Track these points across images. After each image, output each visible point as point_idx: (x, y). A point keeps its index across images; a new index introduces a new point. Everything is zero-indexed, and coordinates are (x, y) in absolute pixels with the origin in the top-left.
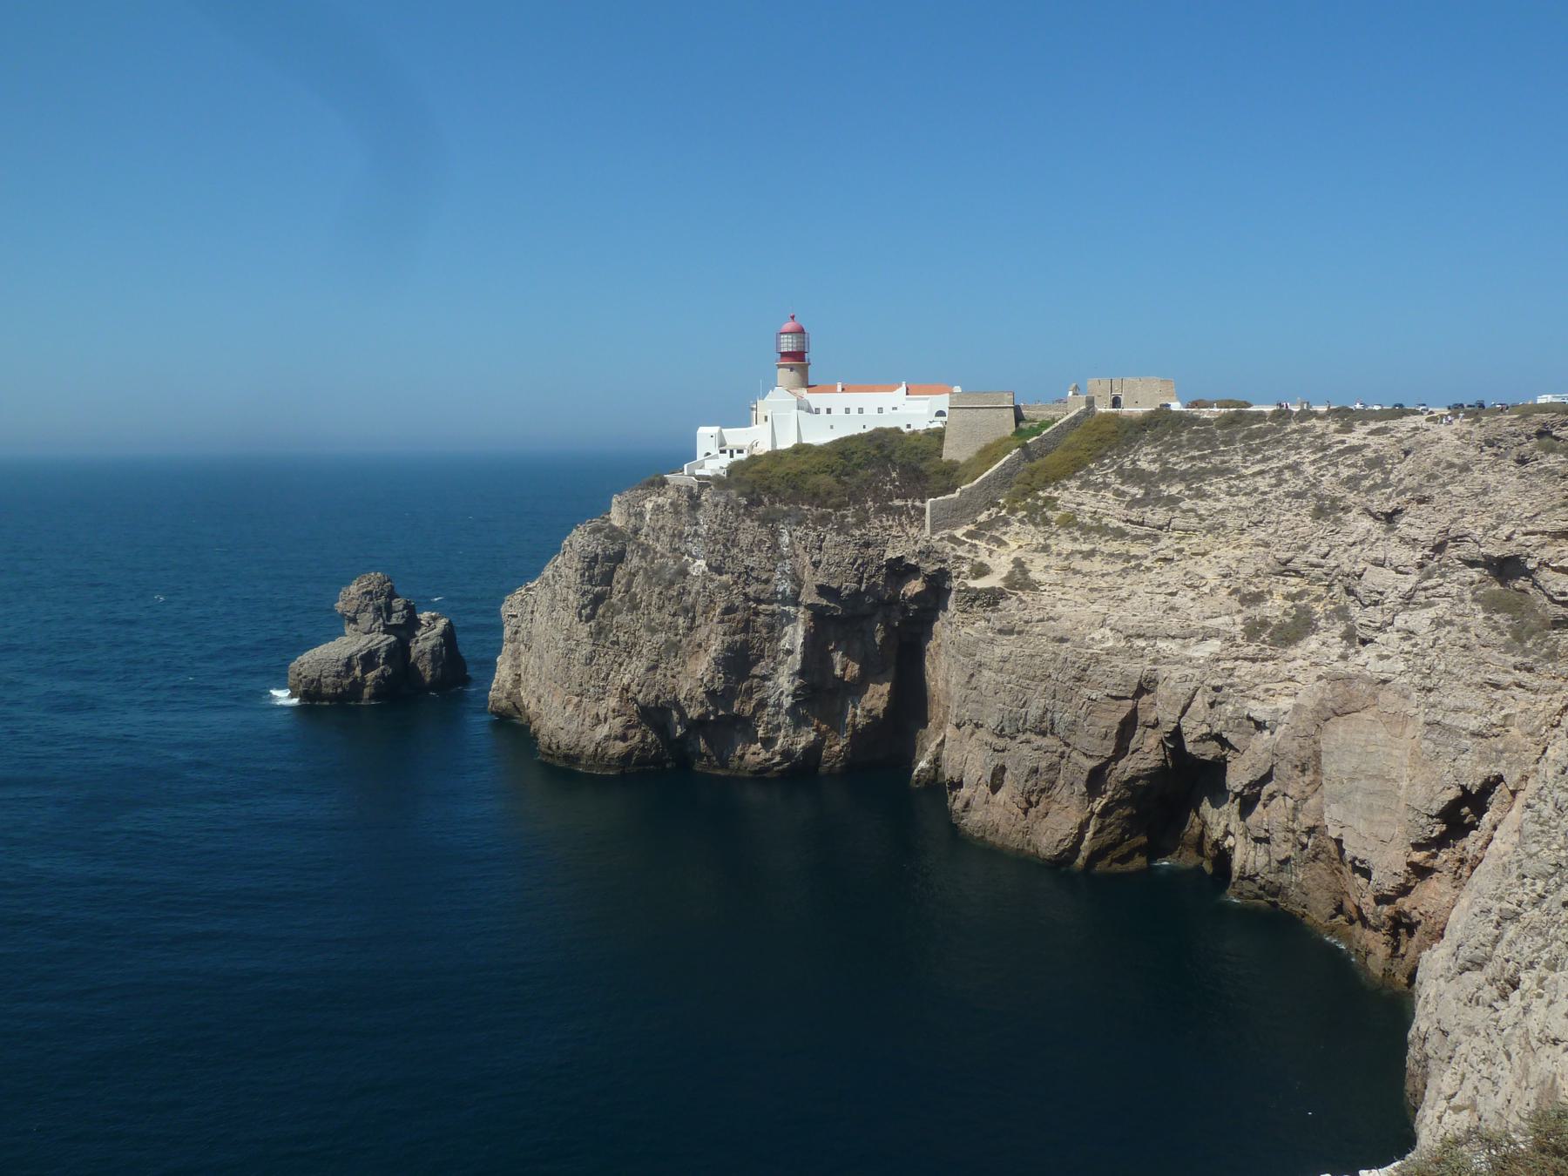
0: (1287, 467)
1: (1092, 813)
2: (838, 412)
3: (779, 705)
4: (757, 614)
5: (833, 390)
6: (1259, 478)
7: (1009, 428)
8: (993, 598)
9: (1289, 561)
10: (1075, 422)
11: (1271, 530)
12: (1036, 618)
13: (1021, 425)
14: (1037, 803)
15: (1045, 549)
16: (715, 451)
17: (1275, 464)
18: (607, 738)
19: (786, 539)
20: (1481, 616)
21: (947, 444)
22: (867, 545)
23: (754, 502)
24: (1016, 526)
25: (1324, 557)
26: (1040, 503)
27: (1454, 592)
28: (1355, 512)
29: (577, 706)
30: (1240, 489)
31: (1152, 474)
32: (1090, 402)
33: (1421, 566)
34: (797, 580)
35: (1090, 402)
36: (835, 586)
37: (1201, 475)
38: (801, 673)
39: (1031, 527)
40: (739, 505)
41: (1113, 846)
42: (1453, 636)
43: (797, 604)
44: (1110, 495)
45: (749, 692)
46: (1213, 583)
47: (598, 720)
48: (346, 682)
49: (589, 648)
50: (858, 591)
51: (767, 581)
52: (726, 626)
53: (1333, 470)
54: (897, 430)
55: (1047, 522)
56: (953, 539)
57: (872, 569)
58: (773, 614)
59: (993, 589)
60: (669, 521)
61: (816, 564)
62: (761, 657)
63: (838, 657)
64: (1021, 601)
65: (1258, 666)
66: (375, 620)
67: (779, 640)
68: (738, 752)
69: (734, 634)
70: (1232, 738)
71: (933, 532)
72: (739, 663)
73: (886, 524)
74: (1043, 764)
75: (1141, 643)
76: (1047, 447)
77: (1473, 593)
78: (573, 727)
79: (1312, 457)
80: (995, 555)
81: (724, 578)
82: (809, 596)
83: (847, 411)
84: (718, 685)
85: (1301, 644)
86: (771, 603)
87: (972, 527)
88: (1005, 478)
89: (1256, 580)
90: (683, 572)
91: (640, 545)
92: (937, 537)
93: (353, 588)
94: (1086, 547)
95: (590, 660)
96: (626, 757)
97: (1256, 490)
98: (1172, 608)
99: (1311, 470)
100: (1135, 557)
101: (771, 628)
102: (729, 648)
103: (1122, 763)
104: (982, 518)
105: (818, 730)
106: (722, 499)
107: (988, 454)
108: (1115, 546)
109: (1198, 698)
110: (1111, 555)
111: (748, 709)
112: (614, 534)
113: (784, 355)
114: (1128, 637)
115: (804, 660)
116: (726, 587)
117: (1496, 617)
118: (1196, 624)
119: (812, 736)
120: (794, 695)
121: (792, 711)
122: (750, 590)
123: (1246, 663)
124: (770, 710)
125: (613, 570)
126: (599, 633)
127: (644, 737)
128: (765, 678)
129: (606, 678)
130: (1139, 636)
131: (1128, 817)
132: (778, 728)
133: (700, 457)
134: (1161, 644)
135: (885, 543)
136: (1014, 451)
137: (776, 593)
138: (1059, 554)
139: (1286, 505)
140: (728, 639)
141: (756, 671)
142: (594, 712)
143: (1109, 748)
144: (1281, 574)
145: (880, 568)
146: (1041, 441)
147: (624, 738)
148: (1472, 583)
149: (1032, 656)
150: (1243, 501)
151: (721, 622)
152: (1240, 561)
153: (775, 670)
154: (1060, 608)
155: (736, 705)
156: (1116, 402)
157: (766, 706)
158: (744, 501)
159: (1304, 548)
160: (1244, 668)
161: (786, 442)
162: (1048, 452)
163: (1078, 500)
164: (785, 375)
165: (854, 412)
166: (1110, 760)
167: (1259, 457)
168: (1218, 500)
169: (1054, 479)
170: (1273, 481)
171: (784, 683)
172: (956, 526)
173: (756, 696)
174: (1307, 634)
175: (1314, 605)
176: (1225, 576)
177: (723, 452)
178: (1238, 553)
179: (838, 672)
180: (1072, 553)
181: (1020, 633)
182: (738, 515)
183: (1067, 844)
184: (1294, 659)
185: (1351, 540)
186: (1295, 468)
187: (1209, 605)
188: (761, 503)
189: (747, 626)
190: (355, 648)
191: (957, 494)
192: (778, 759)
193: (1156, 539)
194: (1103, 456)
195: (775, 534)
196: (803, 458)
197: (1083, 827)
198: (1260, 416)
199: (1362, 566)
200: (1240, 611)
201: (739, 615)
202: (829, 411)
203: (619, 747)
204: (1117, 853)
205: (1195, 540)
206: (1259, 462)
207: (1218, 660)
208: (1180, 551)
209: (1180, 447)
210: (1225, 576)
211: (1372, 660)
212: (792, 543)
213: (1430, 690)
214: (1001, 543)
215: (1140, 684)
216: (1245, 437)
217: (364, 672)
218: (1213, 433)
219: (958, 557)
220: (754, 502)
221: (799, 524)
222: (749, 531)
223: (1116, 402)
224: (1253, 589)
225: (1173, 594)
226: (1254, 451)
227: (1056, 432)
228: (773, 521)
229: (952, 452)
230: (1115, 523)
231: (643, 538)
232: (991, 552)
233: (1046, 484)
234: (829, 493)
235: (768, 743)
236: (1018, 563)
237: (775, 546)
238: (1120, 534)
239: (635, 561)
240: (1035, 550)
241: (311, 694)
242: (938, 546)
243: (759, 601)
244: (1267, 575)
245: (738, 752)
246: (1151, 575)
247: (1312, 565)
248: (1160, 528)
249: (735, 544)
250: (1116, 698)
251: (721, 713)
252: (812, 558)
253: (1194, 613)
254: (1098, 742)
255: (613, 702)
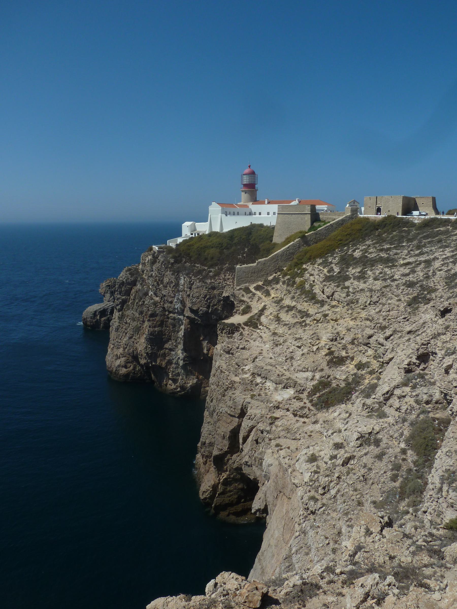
0: (425, 261)
1: (219, 480)
2: (264, 215)
3: (177, 363)
4: (168, 318)
5: (263, 203)
6: (402, 269)
7: (308, 225)
8: (234, 329)
9: (370, 337)
10: (341, 223)
11: (377, 310)
12: (241, 347)
13: (316, 224)
14: (206, 462)
15: (279, 302)
16: (189, 234)
17: (422, 258)
18: (119, 366)
19: (182, 282)
20: (403, 445)
21: (275, 234)
22: (214, 288)
23: (176, 262)
24: (278, 286)
25: (387, 338)
26: (299, 272)
27: (404, 408)
28: (431, 304)
29: (112, 349)
30: (385, 274)
31: (356, 258)
32: (355, 211)
33: (408, 371)
34: (183, 303)
35: (355, 211)
36: (195, 308)
37: (373, 263)
38: (185, 350)
39: (285, 286)
40: (169, 262)
41: (231, 504)
42: (365, 460)
43: (184, 316)
44: (326, 270)
45: (164, 355)
46: (323, 343)
47: (118, 358)
48: (94, 321)
49: (117, 324)
50: (207, 312)
51: (171, 302)
52: (150, 323)
53: (451, 265)
54: (261, 226)
55: (294, 283)
56: (247, 290)
57: (215, 301)
58: (174, 319)
59: (233, 325)
60: (148, 268)
61: (189, 296)
62: (169, 339)
63: (205, 344)
64: (241, 334)
65: (297, 418)
66: (111, 297)
67: (178, 332)
68: (165, 383)
69: (155, 327)
70: (258, 473)
71: (238, 285)
72: (157, 341)
73: (227, 277)
74: (207, 442)
75: (259, 380)
76: (318, 238)
77: (418, 415)
78: (110, 358)
79: (449, 254)
80: (260, 301)
81: (157, 299)
82: (187, 313)
83: (268, 214)
84: (149, 351)
85: (331, 410)
86: (174, 313)
87: (260, 283)
88: (288, 255)
89: (350, 346)
90: (146, 294)
91: (143, 278)
92: (238, 288)
93: (104, 284)
94: (294, 304)
95: (117, 330)
96: (126, 376)
97: (393, 276)
98: (292, 358)
99: (437, 264)
100: (308, 315)
101: (174, 326)
102: (151, 334)
103: (234, 456)
104: (270, 278)
105: (197, 378)
106: (162, 260)
107: (288, 240)
108: (304, 306)
109: (252, 433)
110: (300, 311)
111: (164, 364)
112: (134, 273)
113: (245, 185)
114: (253, 374)
115: (184, 345)
116: (155, 304)
117: (410, 452)
118: (287, 374)
119: (195, 381)
120: (184, 360)
121: (184, 367)
122: (166, 306)
123: (292, 416)
124: (174, 365)
125: (131, 289)
126: (121, 318)
127: (134, 368)
128: (171, 350)
129: (121, 339)
130: (259, 375)
131: (242, 489)
132: (178, 374)
133: (183, 235)
134: (268, 384)
135: (223, 288)
136: (297, 240)
137: (175, 309)
138: (280, 307)
139: (400, 291)
140: (151, 329)
141: (167, 346)
142: (115, 353)
143: (225, 445)
144: (367, 344)
145: (219, 301)
146: (316, 234)
147: (126, 367)
148: (427, 403)
149: (221, 371)
150: (379, 284)
151: (149, 321)
152: (349, 330)
153: (176, 346)
154: (257, 343)
155: (158, 361)
156: (379, 210)
157: (171, 363)
158: (172, 261)
159: (383, 328)
160: (287, 419)
161: (216, 229)
162: (320, 240)
163: (313, 272)
164: (244, 196)
165: (271, 213)
166: (226, 453)
167: (417, 252)
168: (365, 283)
169: (311, 259)
170: (407, 271)
171: (179, 353)
172: (253, 282)
173: (167, 358)
174: (341, 401)
175: (368, 376)
176: (332, 340)
177: (192, 234)
178: (352, 323)
179: (205, 351)
180: (284, 307)
181: (232, 354)
182: (166, 268)
183: (206, 495)
184: (315, 422)
185: (408, 329)
186: (428, 263)
187: (308, 362)
188: (182, 261)
189: (162, 324)
190: (100, 307)
191: (255, 264)
192: (179, 389)
193: (322, 303)
194: (345, 245)
195: (178, 279)
196: (211, 239)
197: (215, 487)
198: (448, 221)
199: (391, 356)
200: (322, 370)
201: (158, 318)
202: (260, 214)
203: (123, 371)
204: (233, 509)
205: (337, 310)
206: (417, 255)
207: (278, 408)
208: (326, 316)
209: (385, 241)
210: (332, 340)
211: (303, 458)
212: (184, 284)
213: (313, 513)
214: (268, 294)
215: (242, 409)
216: (421, 238)
217: (101, 317)
218: (408, 232)
219: (244, 301)
220: (176, 261)
221: (187, 275)
222: (168, 277)
223: (379, 210)
224: (344, 354)
225: (299, 347)
226: (418, 247)
227: (327, 229)
228: (178, 272)
229: (277, 239)
230: (317, 290)
231: (144, 276)
232: (260, 299)
233: (309, 259)
234: (212, 258)
235: (175, 381)
236: (264, 308)
237: (177, 285)
238: (312, 297)
239: (139, 286)
240: (275, 302)
241: (85, 324)
242: (237, 292)
243: (170, 312)
244: (359, 344)
245: (165, 383)
246: (300, 331)
247: (379, 344)
248: (328, 297)
249: (162, 282)
250: (229, 414)
251: (153, 363)
252: (188, 294)
253: (295, 364)
254: (220, 440)
255: (121, 350)
